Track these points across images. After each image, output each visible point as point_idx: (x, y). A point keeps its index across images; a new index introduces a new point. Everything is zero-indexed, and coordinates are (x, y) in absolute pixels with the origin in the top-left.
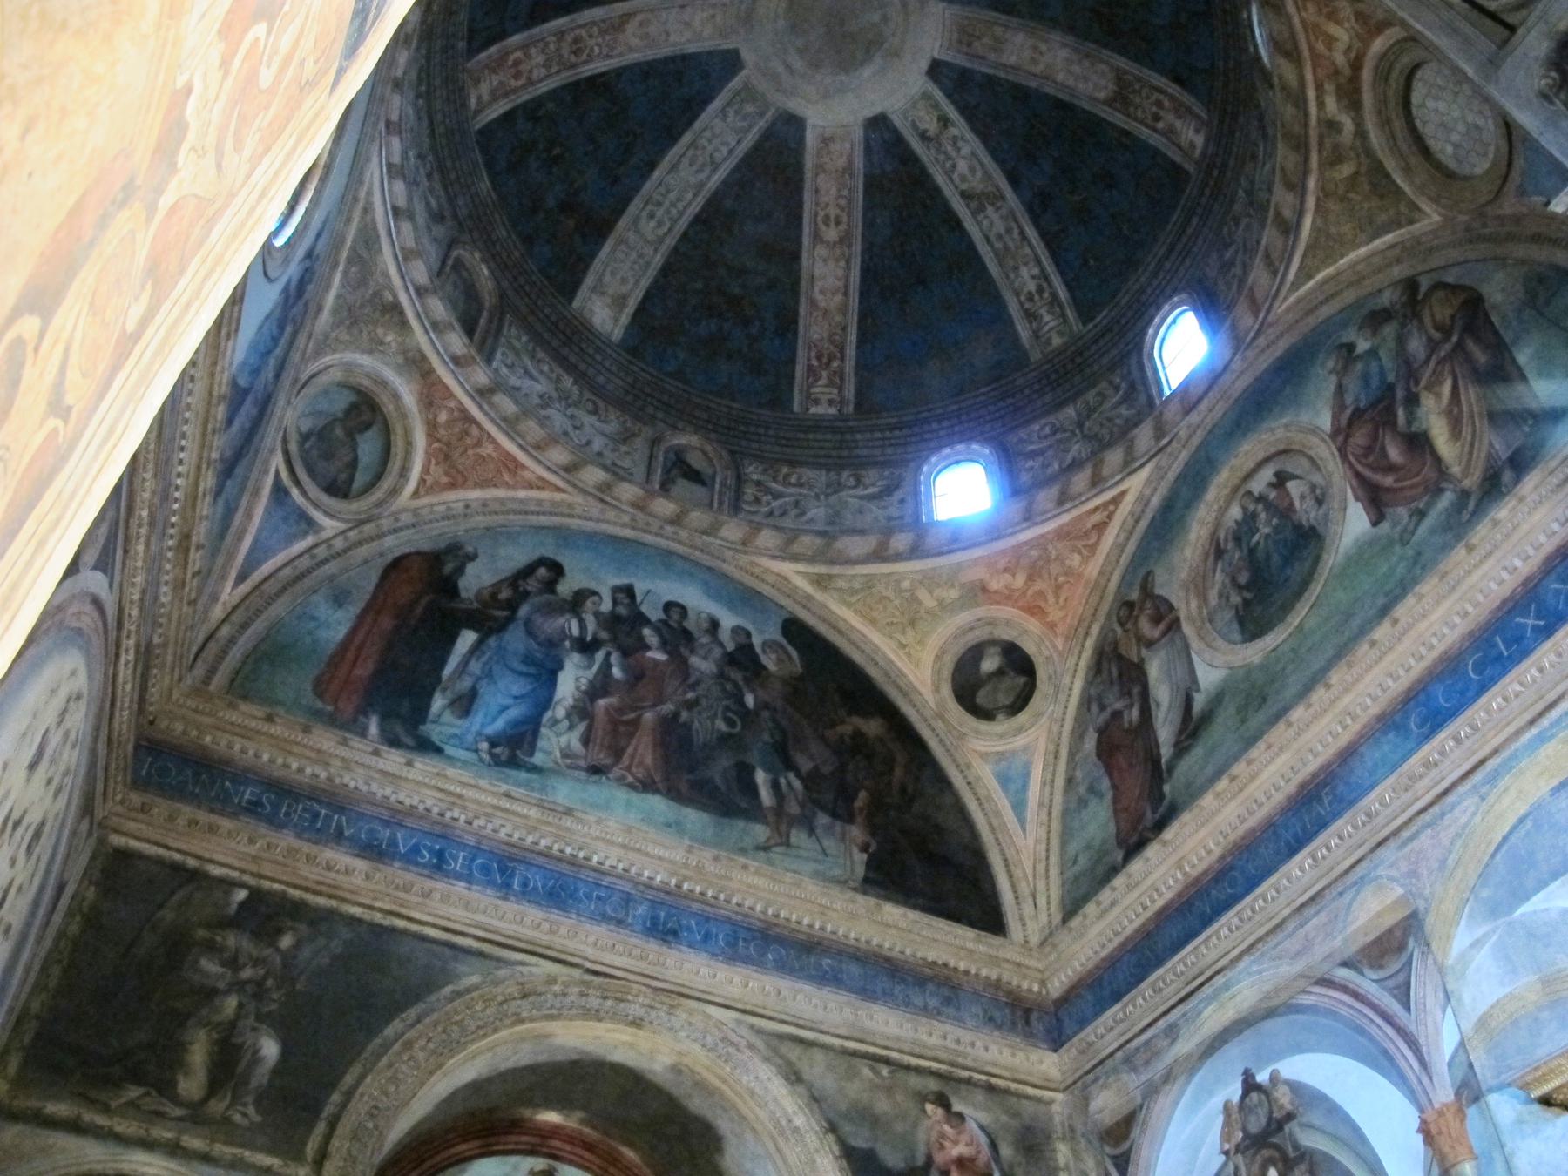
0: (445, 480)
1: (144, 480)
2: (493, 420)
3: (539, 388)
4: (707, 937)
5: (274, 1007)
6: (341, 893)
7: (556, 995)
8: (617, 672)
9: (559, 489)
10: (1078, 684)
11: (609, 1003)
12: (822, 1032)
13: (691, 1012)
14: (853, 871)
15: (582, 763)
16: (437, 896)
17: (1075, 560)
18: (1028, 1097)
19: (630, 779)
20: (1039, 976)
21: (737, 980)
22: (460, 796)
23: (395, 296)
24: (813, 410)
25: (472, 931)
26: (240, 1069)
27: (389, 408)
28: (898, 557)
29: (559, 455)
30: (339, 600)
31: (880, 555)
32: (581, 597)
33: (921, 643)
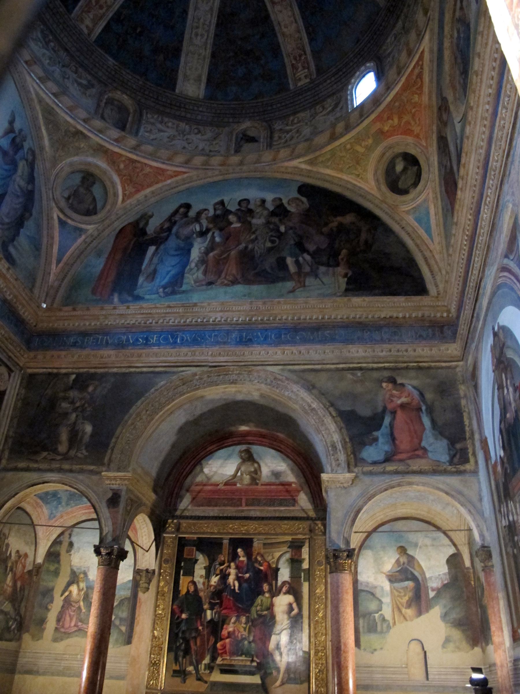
0: (134, 190)
2: (144, 157)
3: (166, 134)
4: (266, 338)
5: (88, 413)
7: (197, 380)
8: (218, 239)
9: (185, 173)
10: (436, 158)
11: (221, 377)
12: (324, 364)
13: (258, 371)
14: (339, 287)
15: (204, 283)
16: (144, 355)
17: (416, 98)
18: (442, 368)
19: (226, 282)
20: (445, 309)
21: (279, 352)
22: (150, 314)
23: (75, 128)
24: (299, 84)
25: (160, 364)
26: (79, 438)
28: (342, 135)
29: (180, 159)
30: (99, 255)
31: (333, 138)
32: (199, 214)
33: (365, 170)
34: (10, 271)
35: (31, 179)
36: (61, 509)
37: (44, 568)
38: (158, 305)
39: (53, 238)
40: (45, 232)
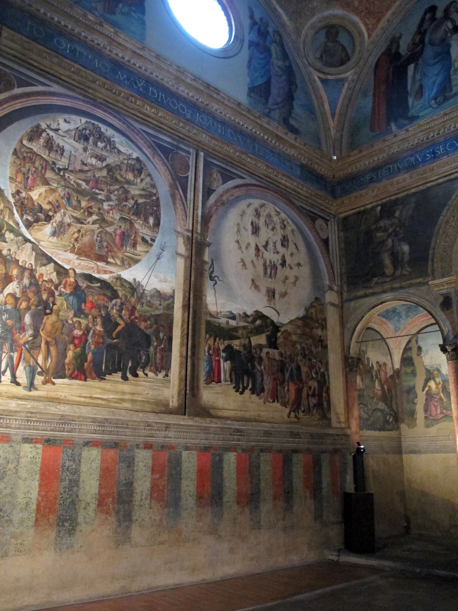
0: (375, 21)
1: (226, 150)
5: (402, 235)
6: (406, 188)
22: (430, 128)
25: (454, 171)
26: (400, 259)
27: (335, 21)
30: (365, 95)
34: (298, 140)
35: (285, 56)
36: (402, 321)
37: (403, 372)
38: (435, 117)
39: (321, 98)
40: (313, 97)
